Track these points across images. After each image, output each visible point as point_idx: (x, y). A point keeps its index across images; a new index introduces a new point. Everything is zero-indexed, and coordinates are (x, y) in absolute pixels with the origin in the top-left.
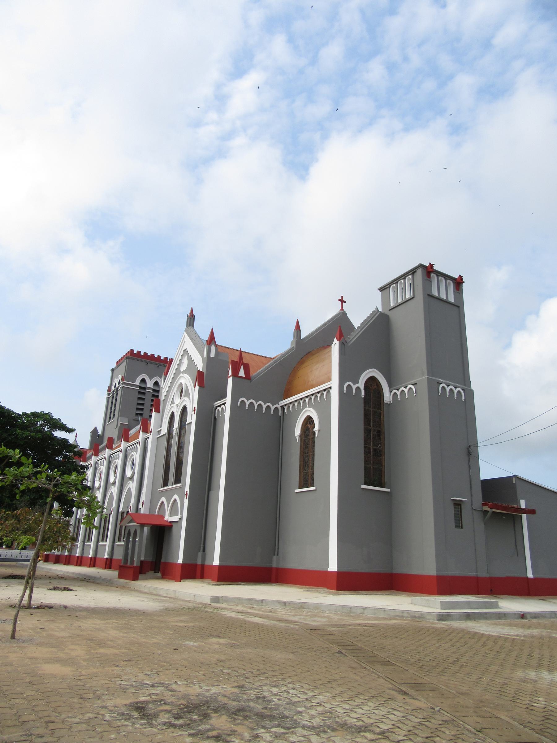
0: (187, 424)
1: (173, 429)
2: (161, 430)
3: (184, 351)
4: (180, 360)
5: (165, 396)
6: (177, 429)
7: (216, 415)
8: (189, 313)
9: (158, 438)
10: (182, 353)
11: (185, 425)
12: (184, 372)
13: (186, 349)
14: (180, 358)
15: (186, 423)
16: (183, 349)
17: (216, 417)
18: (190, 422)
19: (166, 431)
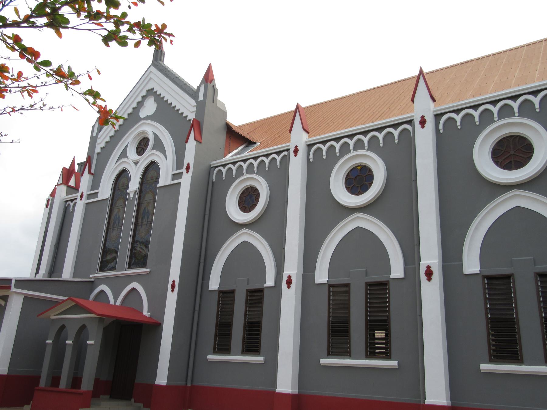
0: (160, 187)
1: (128, 191)
2: (97, 193)
3: (148, 91)
4: (138, 103)
5: (102, 148)
6: (136, 192)
7: (214, 178)
9: (87, 204)
10: (144, 93)
11: (156, 188)
13: (153, 89)
14: (139, 99)
15: (160, 185)
16: (149, 87)
17: (214, 181)
18: (169, 182)
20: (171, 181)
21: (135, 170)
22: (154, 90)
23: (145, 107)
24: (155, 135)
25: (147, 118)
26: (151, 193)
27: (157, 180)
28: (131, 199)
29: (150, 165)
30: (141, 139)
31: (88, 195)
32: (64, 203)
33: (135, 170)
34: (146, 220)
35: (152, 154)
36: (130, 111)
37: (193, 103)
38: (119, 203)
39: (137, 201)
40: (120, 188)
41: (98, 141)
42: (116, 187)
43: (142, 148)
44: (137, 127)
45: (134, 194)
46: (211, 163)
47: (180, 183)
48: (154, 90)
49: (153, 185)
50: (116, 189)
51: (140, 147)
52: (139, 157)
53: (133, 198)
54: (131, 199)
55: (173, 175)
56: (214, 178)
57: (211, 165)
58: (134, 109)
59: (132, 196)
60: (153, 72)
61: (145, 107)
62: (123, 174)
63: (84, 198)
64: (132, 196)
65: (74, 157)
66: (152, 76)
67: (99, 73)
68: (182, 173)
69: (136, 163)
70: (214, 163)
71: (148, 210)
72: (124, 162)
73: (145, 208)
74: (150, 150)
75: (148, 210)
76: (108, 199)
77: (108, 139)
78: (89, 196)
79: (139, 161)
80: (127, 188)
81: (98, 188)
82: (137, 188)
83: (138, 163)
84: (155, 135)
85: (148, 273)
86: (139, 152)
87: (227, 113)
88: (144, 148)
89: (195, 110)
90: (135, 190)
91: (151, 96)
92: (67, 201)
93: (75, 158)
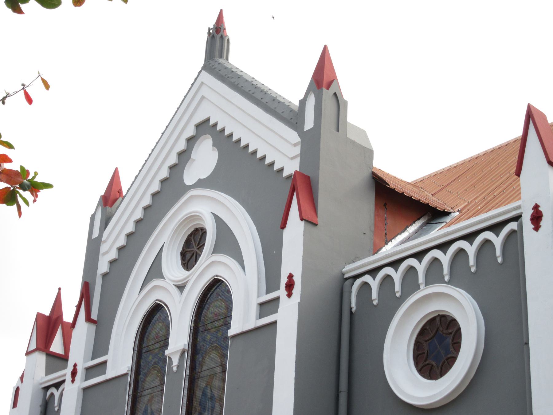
1: (167, 352)
3: (198, 126)
4: (181, 154)
5: (112, 263)
6: (183, 352)
7: (353, 305)
8: (212, 23)
11: (226, 339)
12: (201, 184)
13: (208, 120)
15: (231, 332)
16: (198, 119)
18: (253, 322)
19: (130, 365)
20: (257, 319)
21: (180, 302)
22: (212, 122)
23: (194, 160)
24: (218, 219)
26: (215, 352)
27: (228, 325)
28: (175, 369)
29: (211, 289)
30: (189, 233)
31: (88, 369)
32: (41, 393)
33: (180, 302)
35: (213, 262)
36: (164, 173)
37: (294, 136)
38: (151, 381)
39: (188, 374)
40: (151, 348)
41: (104, 248)
42: (144, 346)
43: (192, 252)
44: (180, 208)
46: (344, 270)
47: (275, 323)
48: (212, 122)
49: (220, 334)
50: (144, 350)
51: (189, 250)
52: (187, 273)
53: (178, 366)
54: (175, 369)
55: (261, 305)
56: (353, 305)
57: (344, 275)
58: (171, 168)
59: (175, 362)
60: (206, 85)
61: (194, 160)
62: (156, 318)
64: (175, 362)
65: (60, 289)
66: (204, 92)
67: (47, 86)
68: (277, 299)
69: (181, 288)
70: (350, 269)
71: (211, 390)
72: (155, 287)
73: (205, 388)
74: (208, 256)
77: (122, 241)
78: (90, 371)
79: (187, 282)
80: (166, 346)
81: (106, 352)
82: (185, 345)
84: (218, 219)
86: (188, 262)
87: (373, 151)
88: (196, 252)
89: (299, 152)
90: (182, 348)
92: (47, 388)
93: (61, 291)
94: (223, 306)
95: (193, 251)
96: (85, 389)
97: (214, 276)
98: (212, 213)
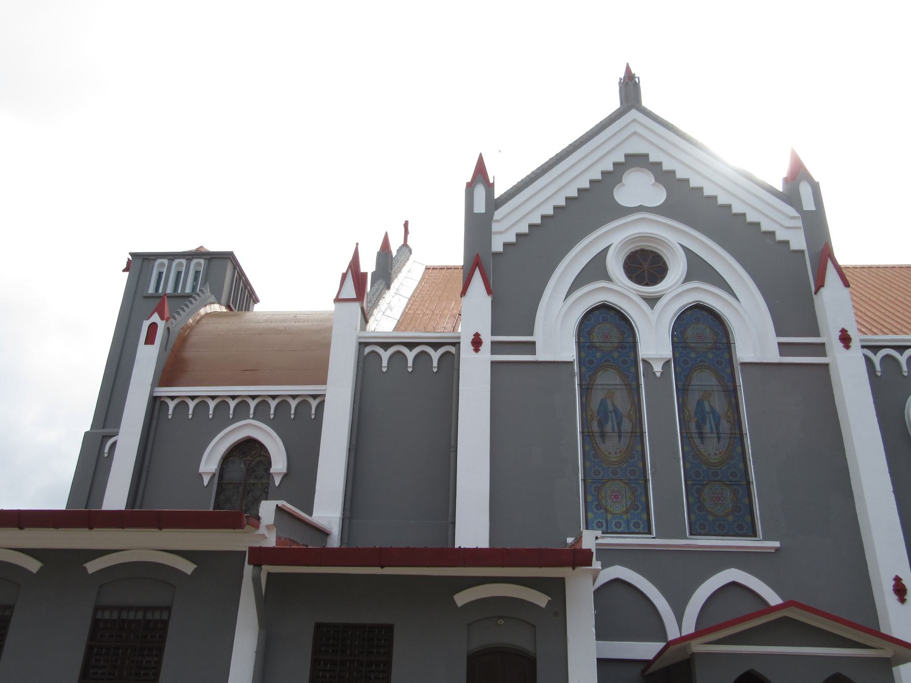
5: (505, 245)
6: (667, 363)
23: (623, 185)
25: (641, 209)
28: (658, 374)
30: (633, 250)
34: (711, 429)
37: (791, 211)
43: (642, 270)
45: (662, 367)
54: (658, 374)
59: (658, 368)
61: (623, 185)
63: (486, 347)
64: (658, 368)
65: (357, 244)
71: (711, 406)
75: (711, 406)
76: (571, 363)
83: (660, 298)
85: (773, 551)
91: (645, 170)
92: (367, 344)
93: (359, 246)
94: (708, 330)
95: (642, 268)
96: (493, 363)
97: (697, 301)
98: (679, 243)
